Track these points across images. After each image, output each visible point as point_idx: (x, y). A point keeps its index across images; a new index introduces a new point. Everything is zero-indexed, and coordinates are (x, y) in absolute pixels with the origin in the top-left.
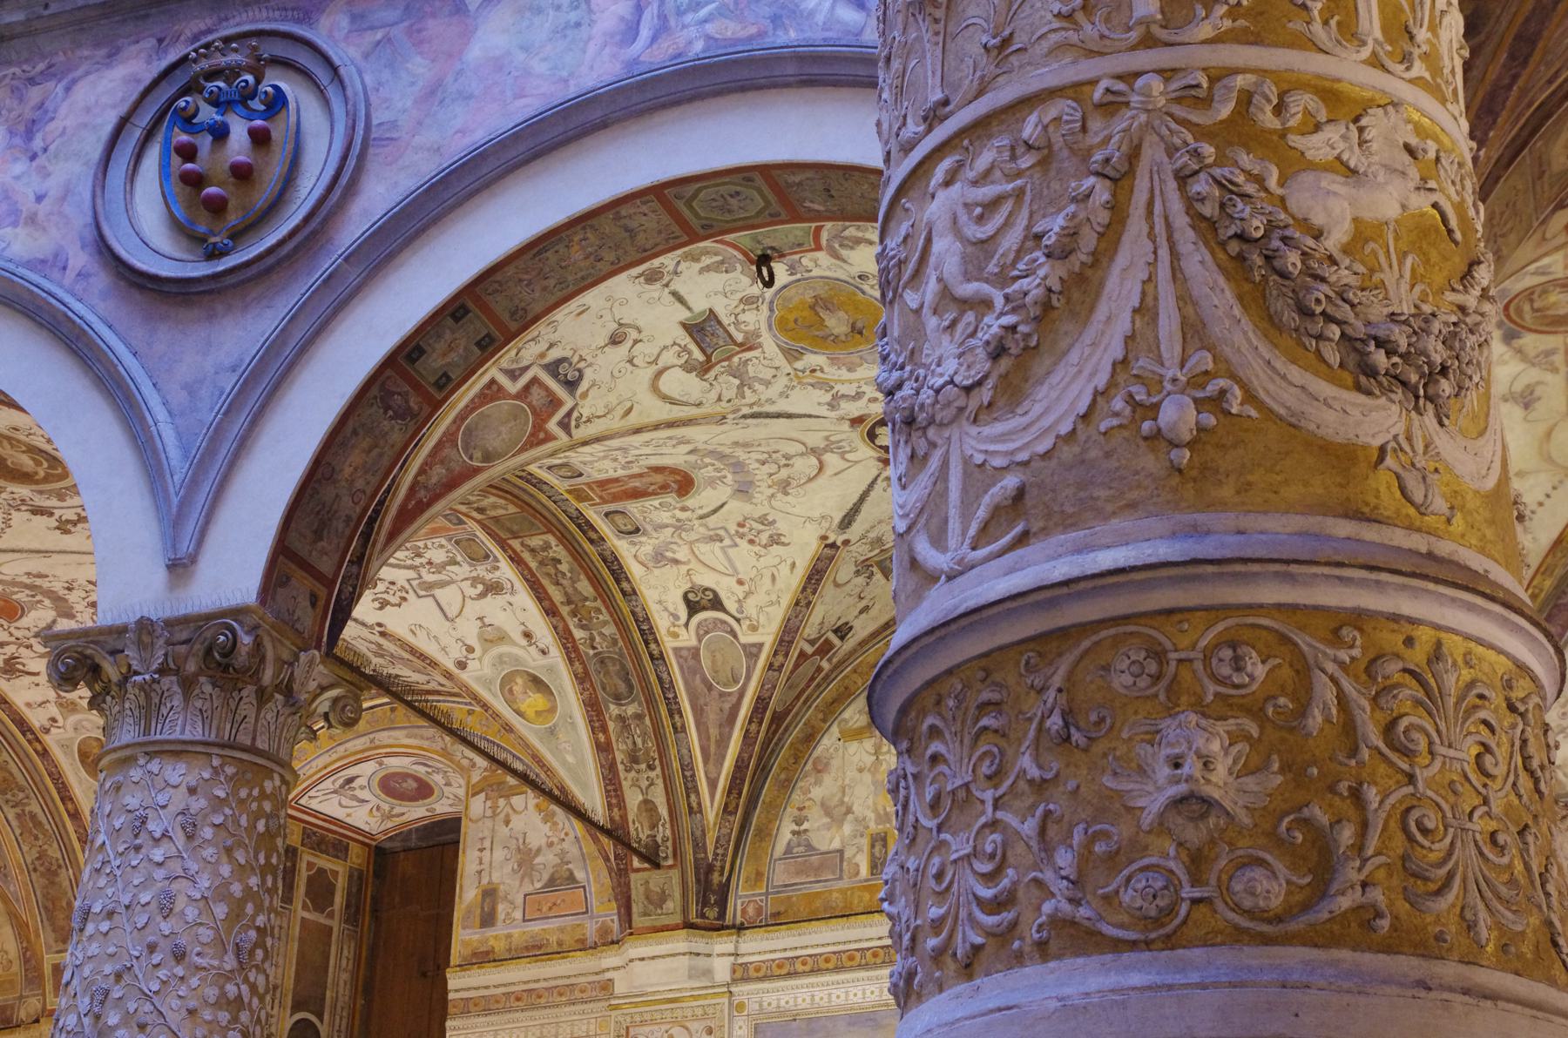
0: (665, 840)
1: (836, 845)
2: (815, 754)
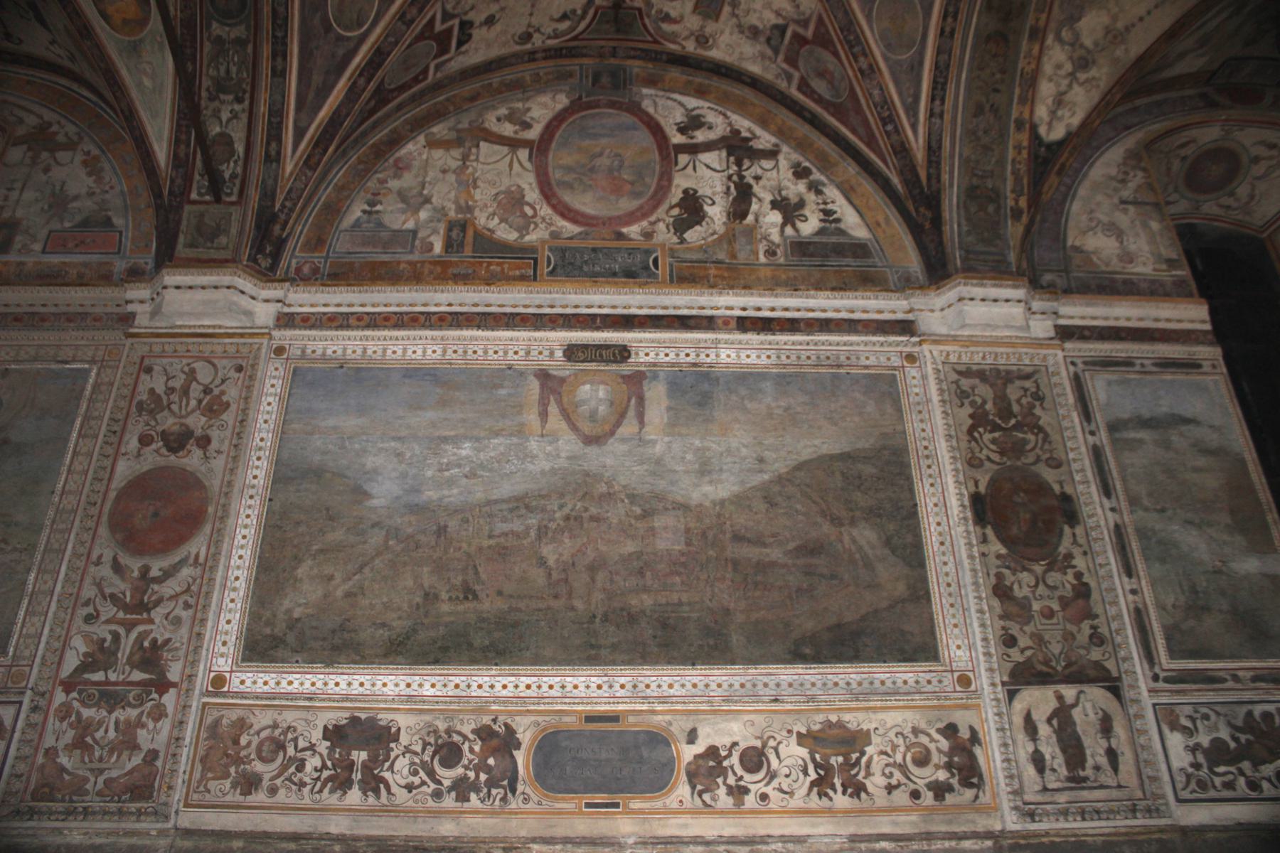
0: (234, 176)
1: (410, 225)
2: (397, 155)
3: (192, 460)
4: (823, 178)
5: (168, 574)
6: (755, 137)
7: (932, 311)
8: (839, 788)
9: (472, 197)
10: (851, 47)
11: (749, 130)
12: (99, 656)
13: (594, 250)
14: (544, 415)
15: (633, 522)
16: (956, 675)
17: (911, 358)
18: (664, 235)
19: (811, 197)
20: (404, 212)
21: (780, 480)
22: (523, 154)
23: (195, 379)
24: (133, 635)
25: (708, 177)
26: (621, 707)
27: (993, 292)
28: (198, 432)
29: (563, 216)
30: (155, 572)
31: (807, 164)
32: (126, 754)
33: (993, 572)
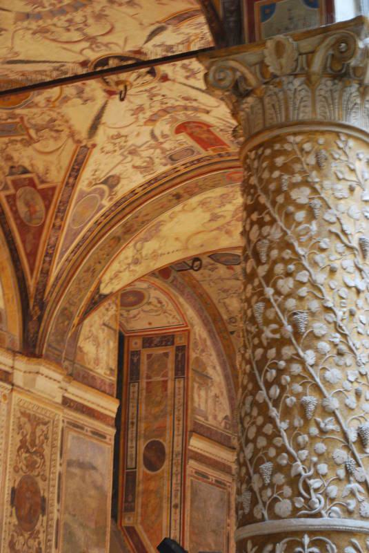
10: (58, 212)
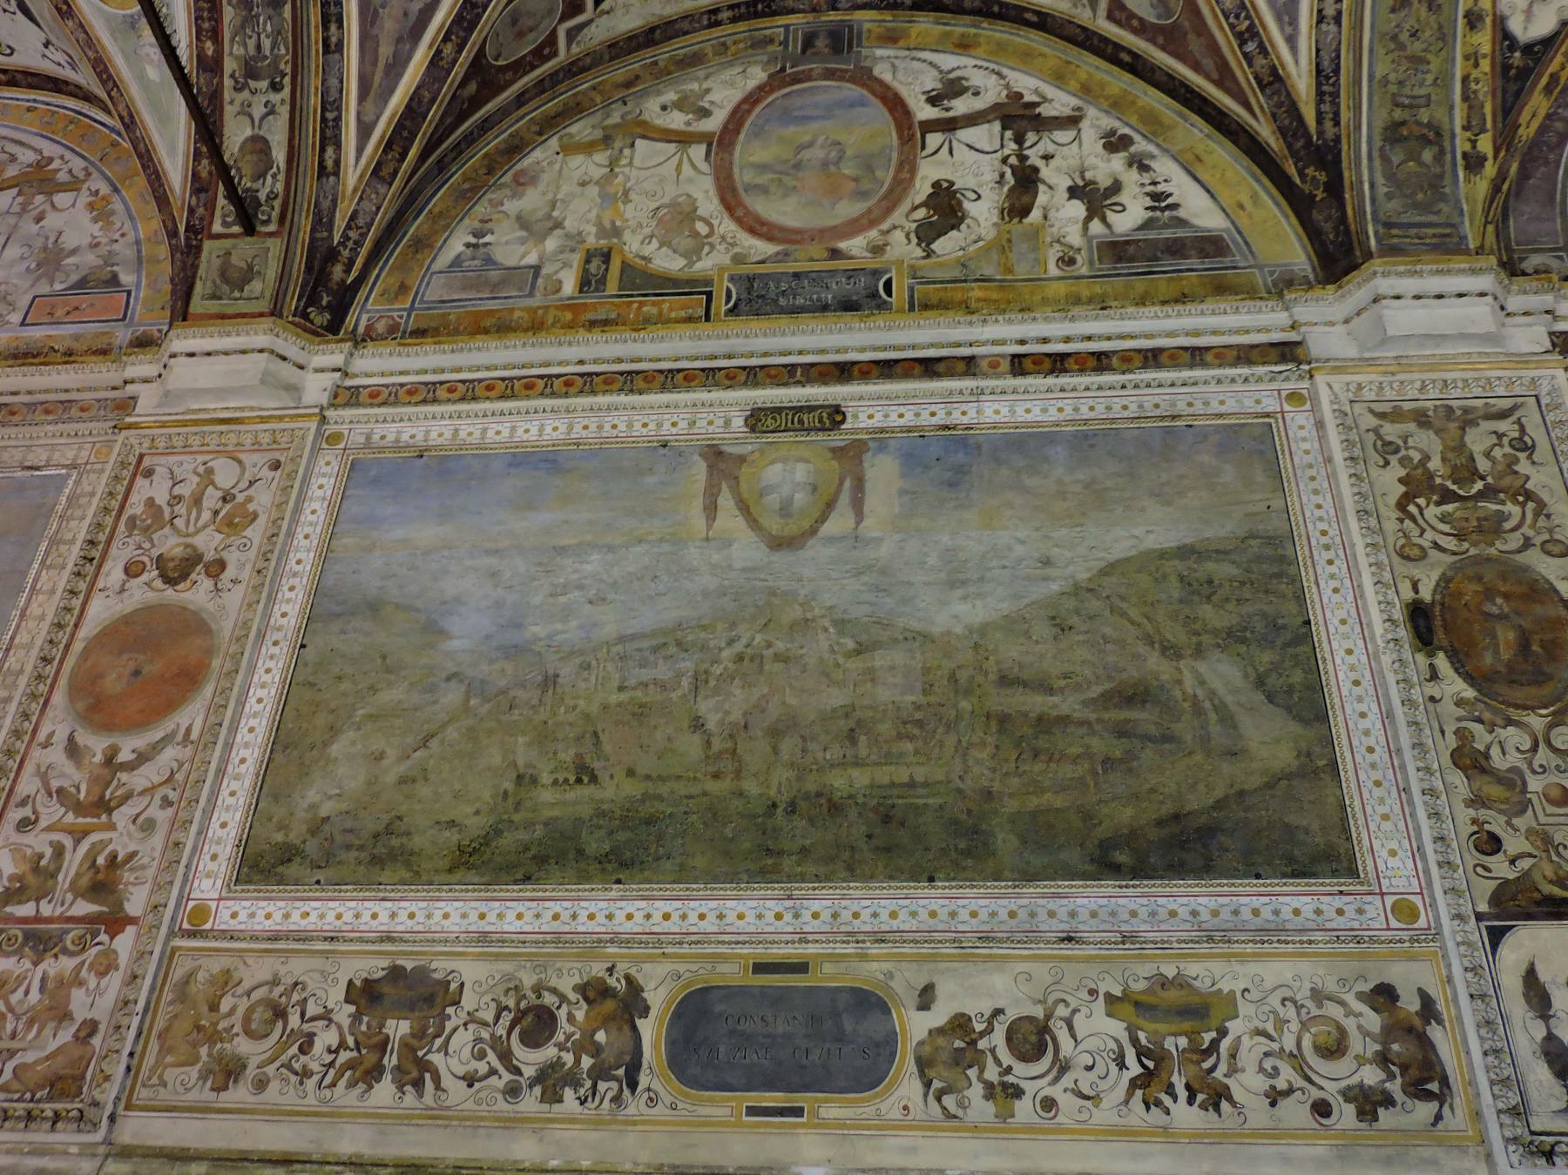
0: (272, 196)
1: (532, 259)
3: (197, 594)
4: (1152, 148)
5: (142, 758)
6: (1045, 100)
7: (1332, 324)
8: (1182, 1094)
9: (622, 216)
11: (1036, 91)
12: (31, 880)
13: (797, 275)
14: (711, 510)
15: (841, 660)
16: (1389, 900)
17: (1295, 397)
18: (903, 248)
19: (1131, 178)
20: (523, 241)
21: (1077, 591)
22: (698, 151)
23: (212, 483)
24: (84, 847)
25: (973, 163)
26: (812, 949)
27: (1435, 284)
28: (209, 556)
29: (752, 231)
30: (125, 756)
31: (1126, 131)
32: (48, 1031)
33: (1450, 729)
